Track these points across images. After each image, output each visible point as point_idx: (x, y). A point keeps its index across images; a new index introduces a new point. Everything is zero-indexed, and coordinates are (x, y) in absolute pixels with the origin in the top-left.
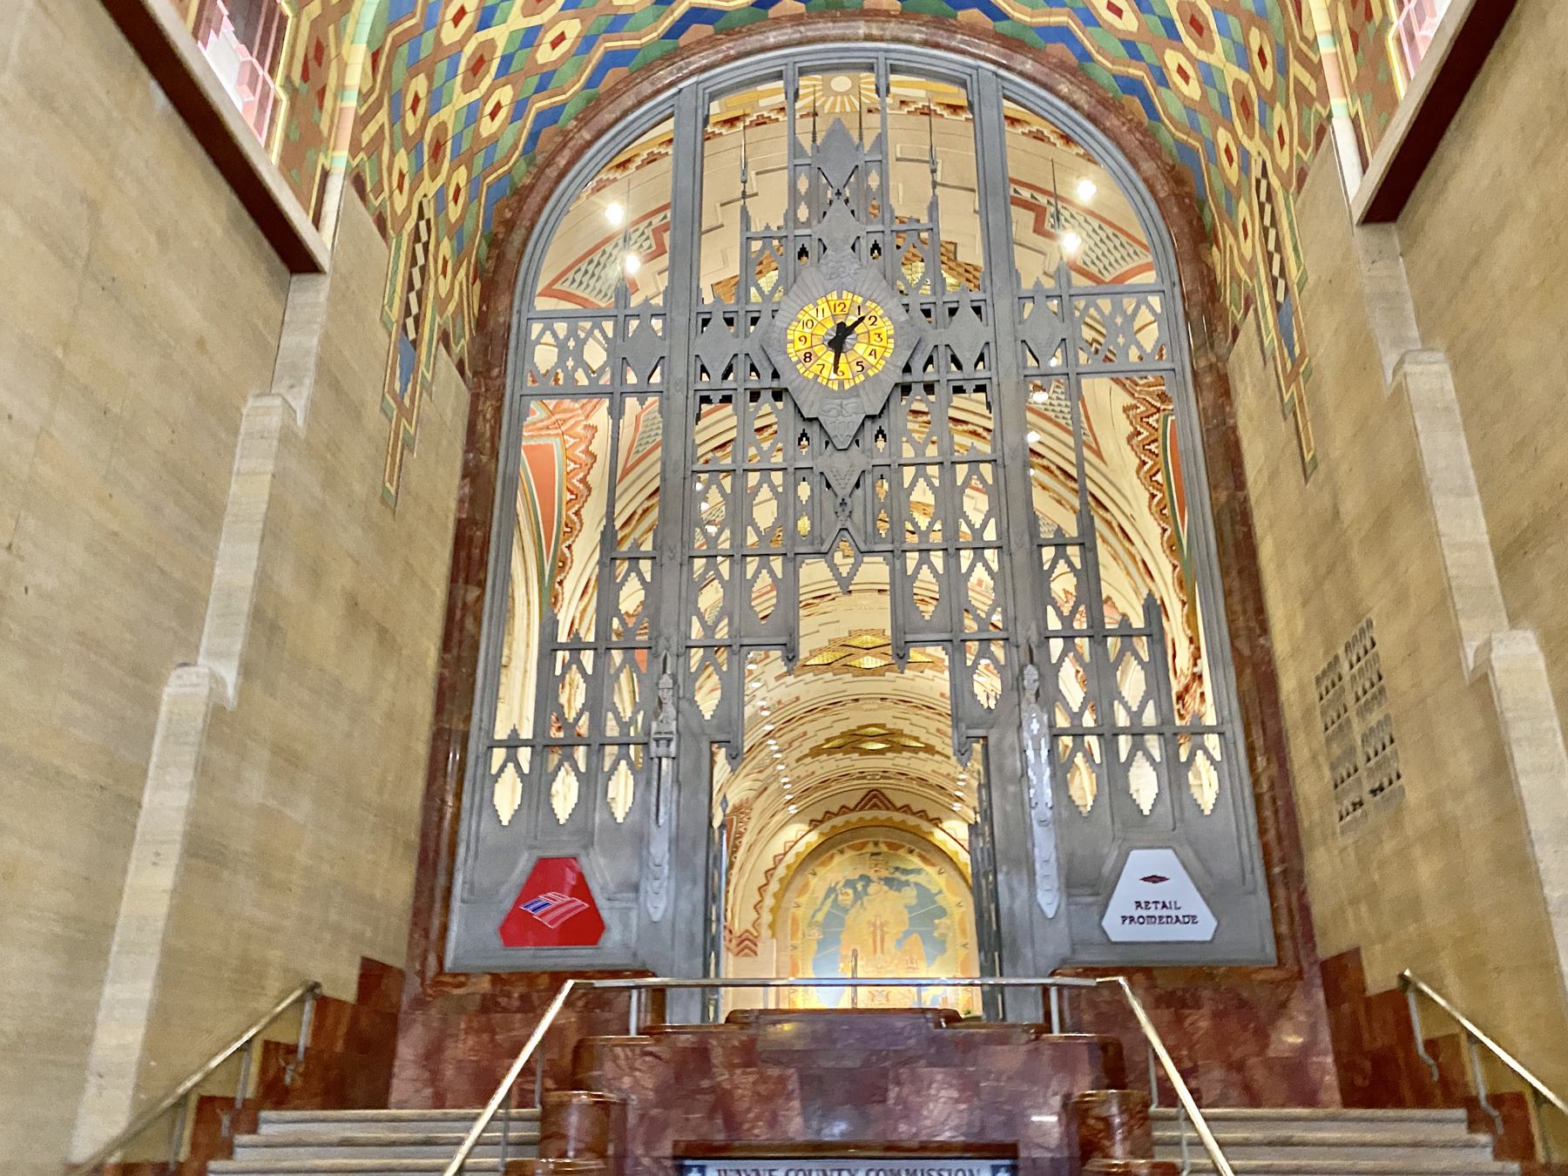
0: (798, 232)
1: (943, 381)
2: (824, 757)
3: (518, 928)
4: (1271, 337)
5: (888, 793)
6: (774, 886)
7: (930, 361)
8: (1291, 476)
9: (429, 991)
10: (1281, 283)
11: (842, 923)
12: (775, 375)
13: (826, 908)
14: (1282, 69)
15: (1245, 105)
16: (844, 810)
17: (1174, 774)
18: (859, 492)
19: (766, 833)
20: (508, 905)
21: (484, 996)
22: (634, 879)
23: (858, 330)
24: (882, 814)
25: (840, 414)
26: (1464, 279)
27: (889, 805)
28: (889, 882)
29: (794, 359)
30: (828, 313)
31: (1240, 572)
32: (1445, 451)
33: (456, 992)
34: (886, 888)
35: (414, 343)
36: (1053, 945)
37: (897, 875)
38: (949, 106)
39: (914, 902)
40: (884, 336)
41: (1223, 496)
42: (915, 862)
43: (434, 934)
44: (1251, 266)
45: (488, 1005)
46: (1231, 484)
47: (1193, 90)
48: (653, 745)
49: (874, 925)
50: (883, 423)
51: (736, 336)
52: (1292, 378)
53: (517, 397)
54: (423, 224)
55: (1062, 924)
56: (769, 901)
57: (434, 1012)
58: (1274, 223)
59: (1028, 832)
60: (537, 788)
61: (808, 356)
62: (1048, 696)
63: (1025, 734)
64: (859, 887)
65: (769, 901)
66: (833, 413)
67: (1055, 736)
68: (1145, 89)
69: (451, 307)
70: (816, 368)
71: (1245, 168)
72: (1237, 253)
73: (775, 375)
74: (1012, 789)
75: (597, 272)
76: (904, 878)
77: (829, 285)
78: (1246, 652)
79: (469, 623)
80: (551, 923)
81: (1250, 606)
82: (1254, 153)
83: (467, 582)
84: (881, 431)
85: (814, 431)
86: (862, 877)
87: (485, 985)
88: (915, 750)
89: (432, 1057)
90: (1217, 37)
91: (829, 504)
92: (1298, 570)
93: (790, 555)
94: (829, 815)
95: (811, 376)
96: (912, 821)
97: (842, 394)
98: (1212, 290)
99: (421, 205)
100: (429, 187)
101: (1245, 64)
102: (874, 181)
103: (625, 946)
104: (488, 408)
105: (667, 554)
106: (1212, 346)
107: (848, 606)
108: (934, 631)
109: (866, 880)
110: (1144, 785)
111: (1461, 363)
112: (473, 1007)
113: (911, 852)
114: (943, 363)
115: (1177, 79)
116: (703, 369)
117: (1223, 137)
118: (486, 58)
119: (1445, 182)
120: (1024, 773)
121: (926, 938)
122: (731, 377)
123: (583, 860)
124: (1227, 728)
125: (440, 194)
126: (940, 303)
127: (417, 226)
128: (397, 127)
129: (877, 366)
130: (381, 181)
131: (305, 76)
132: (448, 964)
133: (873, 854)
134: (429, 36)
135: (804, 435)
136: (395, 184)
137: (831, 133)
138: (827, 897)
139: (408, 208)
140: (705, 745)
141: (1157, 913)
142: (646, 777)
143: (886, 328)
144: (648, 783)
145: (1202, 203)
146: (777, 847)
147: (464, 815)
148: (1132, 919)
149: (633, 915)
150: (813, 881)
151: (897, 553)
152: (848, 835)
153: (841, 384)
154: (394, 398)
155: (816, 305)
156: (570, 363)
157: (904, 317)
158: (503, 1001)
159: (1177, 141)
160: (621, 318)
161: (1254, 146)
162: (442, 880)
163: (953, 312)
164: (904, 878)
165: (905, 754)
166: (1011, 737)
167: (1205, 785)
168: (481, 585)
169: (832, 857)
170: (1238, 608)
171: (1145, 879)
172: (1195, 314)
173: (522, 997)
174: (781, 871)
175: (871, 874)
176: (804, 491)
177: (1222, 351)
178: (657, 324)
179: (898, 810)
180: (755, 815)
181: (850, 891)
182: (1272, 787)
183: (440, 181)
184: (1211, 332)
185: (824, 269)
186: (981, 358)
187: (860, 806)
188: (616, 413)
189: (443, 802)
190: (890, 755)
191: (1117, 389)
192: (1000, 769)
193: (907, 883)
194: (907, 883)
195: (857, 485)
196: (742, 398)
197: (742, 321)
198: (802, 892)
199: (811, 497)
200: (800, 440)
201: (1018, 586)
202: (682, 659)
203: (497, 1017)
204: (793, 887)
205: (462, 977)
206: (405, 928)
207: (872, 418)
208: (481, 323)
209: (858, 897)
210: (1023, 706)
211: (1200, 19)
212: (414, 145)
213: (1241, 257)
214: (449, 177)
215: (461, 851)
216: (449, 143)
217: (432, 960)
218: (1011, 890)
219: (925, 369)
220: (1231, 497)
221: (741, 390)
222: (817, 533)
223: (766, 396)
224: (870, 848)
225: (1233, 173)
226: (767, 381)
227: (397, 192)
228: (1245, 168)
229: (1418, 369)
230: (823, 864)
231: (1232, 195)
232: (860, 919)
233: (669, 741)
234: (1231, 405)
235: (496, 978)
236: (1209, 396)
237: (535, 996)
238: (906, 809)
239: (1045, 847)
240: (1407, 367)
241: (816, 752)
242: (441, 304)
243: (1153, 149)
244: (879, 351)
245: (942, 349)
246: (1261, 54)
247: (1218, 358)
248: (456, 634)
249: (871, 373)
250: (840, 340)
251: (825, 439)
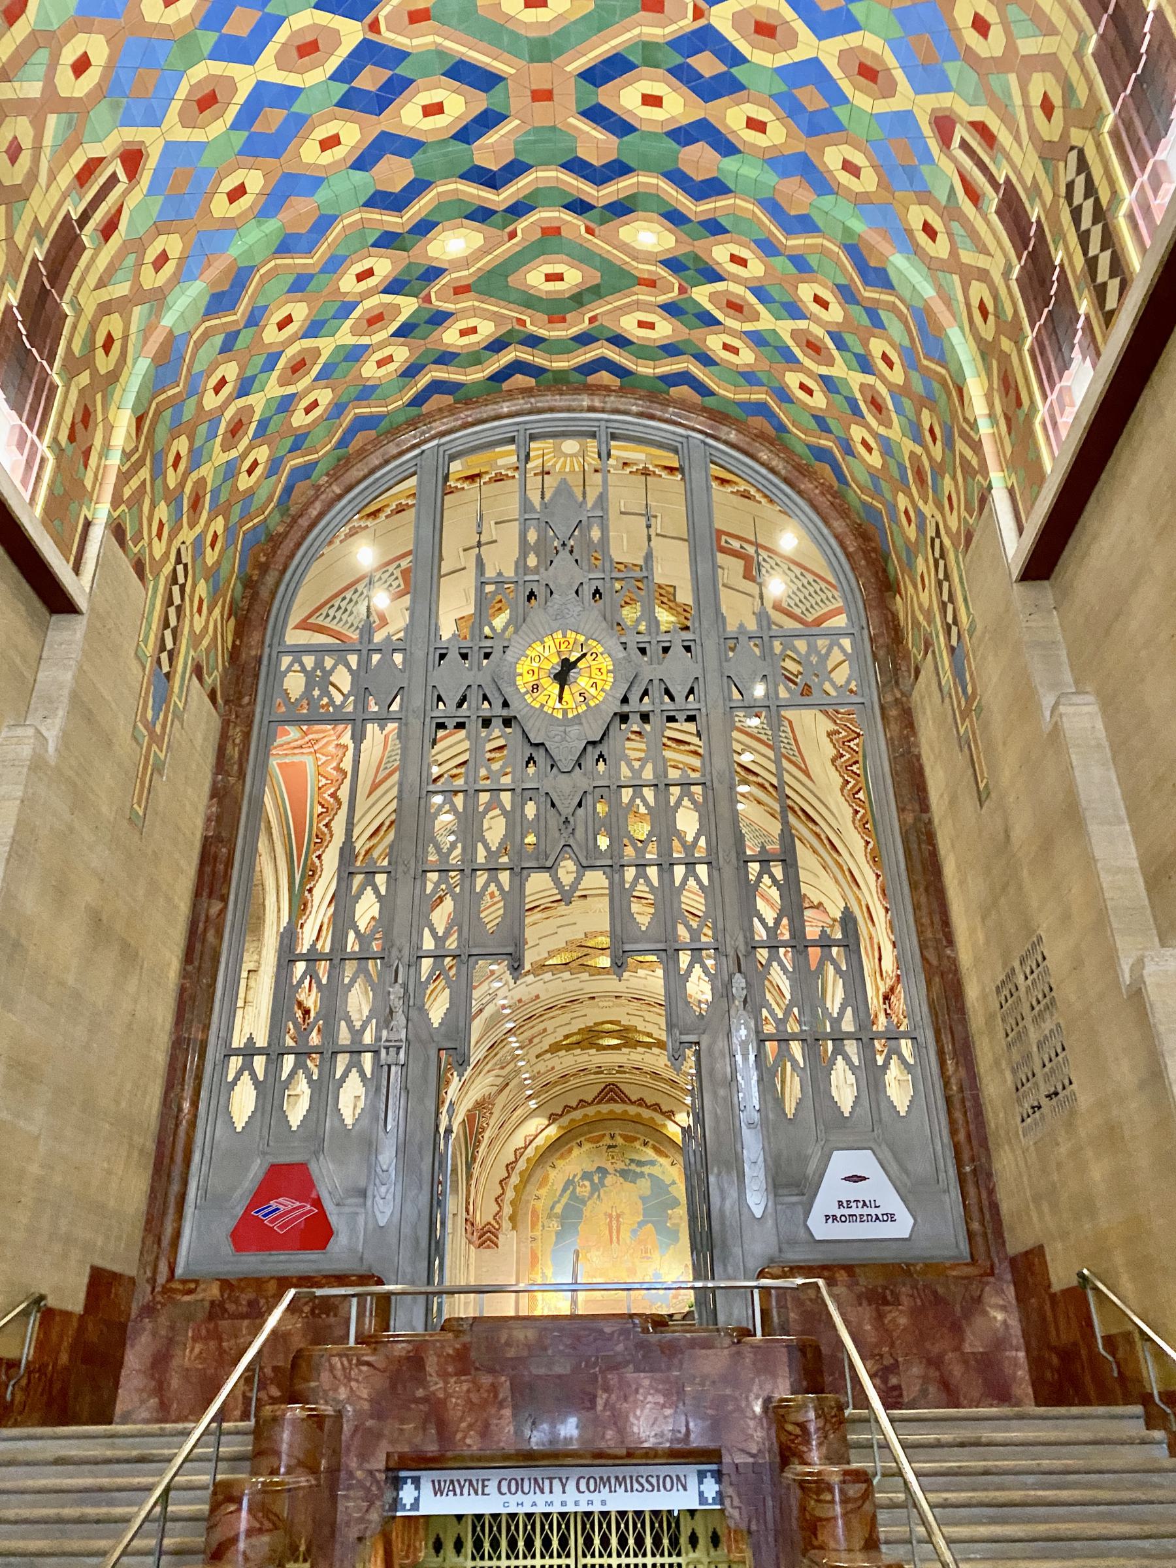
0: (527, 578)
1: (658, 711)
2: (563, 1053)
3: (249, 1233)
4: (947, 678)
5: (626, 1089)
6: (515, 1179)
7: (646, 693)
8: (968, 803)
9: (159, 1298)
10: (954, 629)
11: (579, 1214)
12: (505, 704)
14: (949, 444)
15: (919, 474)
16: (582, 1103)
17: (871, 1079)
18: (580, 811)
19: (508, 1127)
20: (240, 1211)
21: (212, 1303)
22: (362, 1183)
23: (580, 665)
24: (618, 1108)
25: (563, 740)
26: (1107, 632)
27: (625, 1099)
28: (624, 1174)
29: (523, 690)
30: (553, 650)
31: (926, 890)
32: (1097, 782)
33: (187, 1298)
35: (167, 675)
36: (758, 1245)
37: (633, 1167)
38: (666, 468)
39: (648, 1193)
40: (604, 671)
41: (910, 819)
42: (650, 1154)
43: (165, 1242)
44: (929, 615)
45: (216, 1310)
46: (917, 807)
47: (875, 460)
48: (383, 1052)
49: (610, 1216)
50: (604, 748)
51: (470, 669)
52: (965, 714)
53: (265, 722)
54: (180, 568)
55: (770, 1222)
56: (510, 1194)
57: (163, 1320)
58: (947, 577)
59: (737, 1134)
60: (271, 1094)
61: (535, 688)
62: (753, 1003)
63: (735, 1040)
65: (510, 1194)
66: (558, 738)
67: (761, 1041)
68: (835, 459)
69: (205, 643)
70: (542, 699)
71: (921, 529)
72: (917, 600)
73: (505, 704)
74: (722, 1092)
75: (338, 615)
76: (638, 1170)
77: (555, 625)
78: (935, 962)
79: (211, 936)
80: (281, 1227)
81: (937, 919)
82: (929, 516)
83: (210, 896)
84: (601, 756)
85: (539, 755)
87: (215, 1291)
88: (649, 1046)
89: (160, 1363)
90: (894, 416)
91: (554, 822)
92: (977, 886)
93: (517, 870)
94: (567, 1109)
95: (537, 706)
96: (646, 1113)
97: (566, 722)
98: (896, 633)
99: (179, 551)
100: (188, 535)
101: (918, 439)
102: (596, 534)
103: (352, 1250)
104: (237, 733)
105: (401, 868)
106: (897, 683)
107: (570, 917)
108: (649, 940)
109: (602, 1171)
110: (844, 1087)
111: (1108, 705)
112: (201, 1315)
113: (645, 1144)
114: (657, 695)
115: (861, 450)
116: (440, 699)
117: (902, 502)
118: (244, 421)
119: (1089, 546)
120: (734, 1078)
122: (465, 705)
123: (313, 1167)
124: (918, 1034)
125: (198, 542)
126: (654, 642)
127: (175, 570)
128: (159, 481)
129: (597, 697)
130: (141, 531)
131: (72, 438)
132: (179, 1271)
134: (191, 403)
135: (531, 758)
136: (154, 532)
137: (558, 492)
138: (564, 1190)
139: (167, 554)
140: (433, 1053)
141: (858, 1212)
142: (376, 1085)
143: (606, 663)
144: (378, 1089)
145: (886, 558)
146: (518, 1140)
147: (200, 1123)
148: (835, 1218)
149: (361, 1220)
151: (616, 867)
152: (586, 1128)
153: (565, 712)
154: (146, 727)
155: (543, 642)
156: (316, 693)
157: (622, 654)
158: (231, 1307)
159: (864, 503)
160: (365, 652)
161: (928, 509)
162: (175, 1188)
163: (666, 650)
164: (638, 1170)
165: (640, 1049)
166: (721, 1044)
167: (899, 1089)
168: (224, 899)
169: (570, 1151)
170: (925, 920)
171: (846, 1179)
172: (881, 653)
173: (250, 1304)
174: (522, 1165)
175: (608, 1166)
176: (530, 810)
177: (905, 689)
178: (398, 658)
179: (633, 1103)
180: (497, 1110)
181: (587, 1183)
182: (961, 1089)
183: (198, 529)
184: (896, 669)
185: (550, 610)
186: (691, 691)
187: (599, 1099)
188: (359, 738)
189: (180, 1109)
190: (624, 1050)
191: (820, 716)
192: (711, 1073)
193: (642, 1175)
194: (642, 1175)
195: (580, 805)
196: (474, 725)
197: (475, 656)
198: (540, 1187)
199: (537, 816)
200: (528, 763)
201: (727, 901)
202: (412, 970)
203: (224, 1324)
204: (533, 1179)
205: (191, 1284)
206: (138, 1234)
207: (593, 743)
208: (234, 655)
209: (595, 1188)
210: (732, 1012)
211: (880, 401)
212: (174, 498)
213: (921, 606)
214: (207, 525)
215: (196, 1157)
216: (208, 496)
217: (163, 1268)
218: (722, 1191)
219: (641, 700)
220: (917, 819)
221: (474, 717)
222: (542, 847)
223: (497, 723)
224: (607, 1141)
225: (912, 532)
226: (498, 710)
227: (156, 540)
228: (921, 529)
229: (1071, 710)
230: (562, 1157)
231: (912, 551)
232: (597, 1210)
233: (399, 1048)
234: (915, 734)
235: (226, 1284)
236: (895, 727)
237: (262, 1302)
238: (641, 1102)
239: (752, 1148)
240: (1062, 709)
241: (555, 1048)
242: (195, 640)
243: (844, 512)
244: (600, 684)
245: (656, 682)
246: (931, 431)
247: (903, 694)
248: (198, 946)
249: (592, 704)
250: (564, 673)
251: (549, 762)
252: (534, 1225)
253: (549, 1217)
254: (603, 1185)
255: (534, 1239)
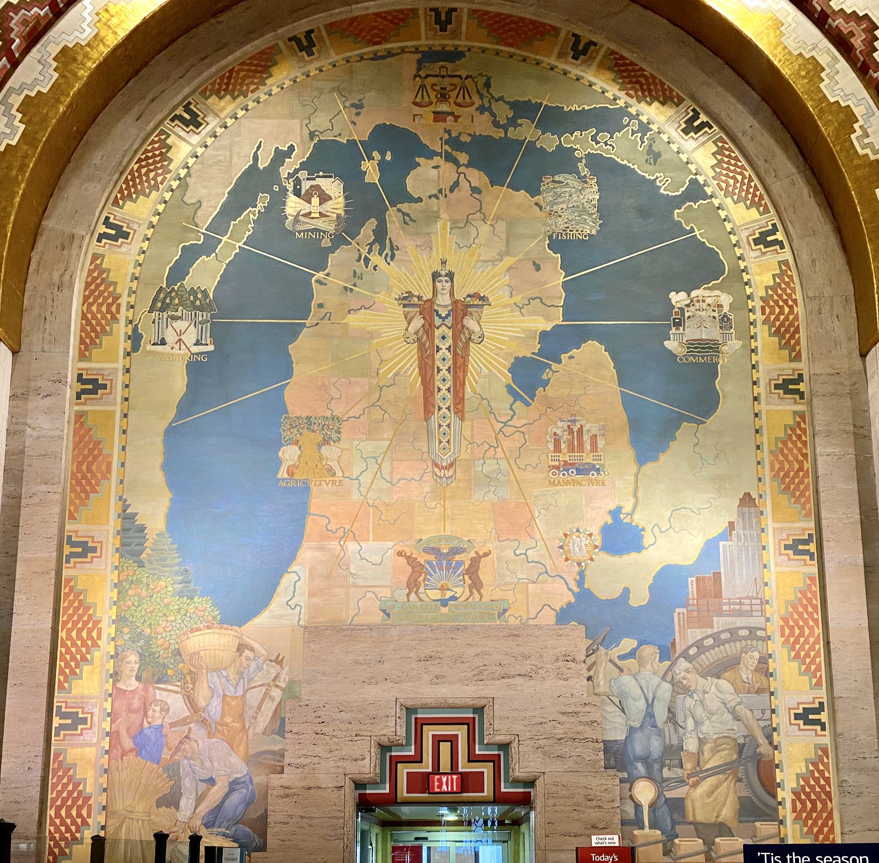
11: (297, 302)
13: (231, 245)
34: (477, 177)
49: (427, 309)
64: (371, 170)
86: (385, 136)
109: (400, 146)
121: (635, 359)
133: (429, 56)
150: (183, 146)
209: (367, 208)
252: (92, 336)
253: (162, 304)
254: (401, 195)
255: (91, 386)
